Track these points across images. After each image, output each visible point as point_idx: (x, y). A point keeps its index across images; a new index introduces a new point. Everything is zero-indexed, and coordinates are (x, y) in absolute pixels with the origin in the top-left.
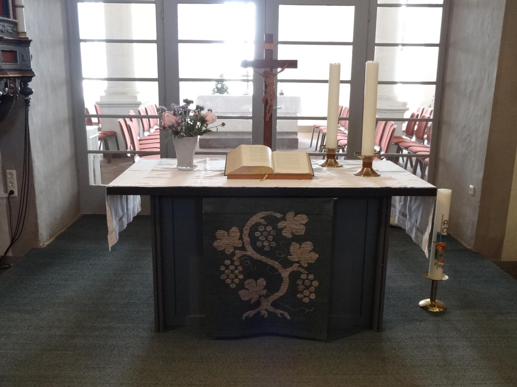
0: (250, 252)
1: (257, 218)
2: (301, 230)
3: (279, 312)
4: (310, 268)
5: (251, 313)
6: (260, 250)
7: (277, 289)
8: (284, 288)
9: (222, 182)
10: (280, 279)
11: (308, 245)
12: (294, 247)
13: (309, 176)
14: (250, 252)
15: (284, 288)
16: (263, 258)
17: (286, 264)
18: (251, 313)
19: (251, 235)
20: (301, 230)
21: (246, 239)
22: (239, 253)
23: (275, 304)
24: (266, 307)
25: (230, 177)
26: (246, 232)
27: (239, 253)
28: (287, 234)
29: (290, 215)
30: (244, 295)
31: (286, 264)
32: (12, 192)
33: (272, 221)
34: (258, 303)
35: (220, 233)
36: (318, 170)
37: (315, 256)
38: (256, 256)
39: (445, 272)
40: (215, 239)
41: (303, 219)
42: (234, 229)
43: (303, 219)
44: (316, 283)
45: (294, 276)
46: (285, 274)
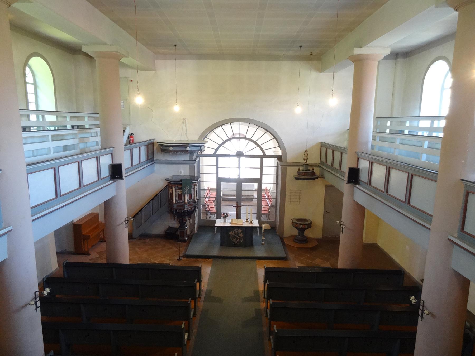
0: (234, 235)
1: (235, 230)
2: (241, 232)
3: (238, 243)
4: (242, 237)
5: (234, 243)
6: (235, 235)
7: (238, 239)
8: (239, 239)
9: (230, 225)
10: (238, 239)
11: (242, 234)
12: (240, 234)
13: (242, 224)
14: (234, 235)
15: (239, 239)
16: (236, 236)
17: (239, 236)
18: (234, 243)
19: (234, 232)
20: (241, 232)
21: (233, 233)
22: (232, 235)
23: (237, 242)
24: (236, 242)
25: (231, 224)
26: (233, 232)
27: (232, 235)
28: (239, 232)
29: (239, 230)
30: (233, 241)
31: (239, 236)
32: (191, 223)
33: (237, 231)
34: (235, 242)
35: (230, 232)
36: (245, 222)
37: (243, 235)
38: (235, 235)
39: (264, 238)
40: (229, 233)
41: (241, 230)
42: (232, 232)
43: (241, 230)
44: (243, 239)
45: (240, 238)
46: (239, 238)
